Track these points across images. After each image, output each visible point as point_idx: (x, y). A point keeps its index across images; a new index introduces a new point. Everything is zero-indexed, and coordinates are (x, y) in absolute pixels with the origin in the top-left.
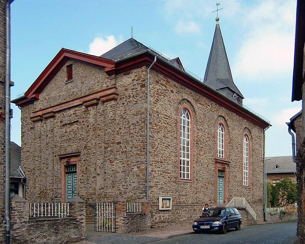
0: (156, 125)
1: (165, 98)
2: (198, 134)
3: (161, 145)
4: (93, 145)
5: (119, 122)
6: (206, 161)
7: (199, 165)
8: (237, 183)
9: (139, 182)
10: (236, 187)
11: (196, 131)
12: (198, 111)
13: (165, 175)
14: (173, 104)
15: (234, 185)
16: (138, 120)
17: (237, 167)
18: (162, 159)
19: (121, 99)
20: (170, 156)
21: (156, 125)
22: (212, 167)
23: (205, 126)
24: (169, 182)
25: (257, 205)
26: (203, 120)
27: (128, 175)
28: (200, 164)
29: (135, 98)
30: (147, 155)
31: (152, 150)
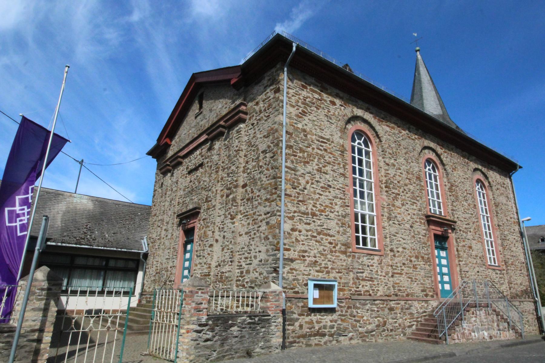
0: (302, 151)
1: (319, 111)
2: (387, 172)
3: (312, 184)
4: (214, 194)
5: (247, 153)
6: (409, 217)
7: (394, 223)
8: (475, 259)
9: (267, 251)
10: (474, 268)
11: (383, 167)
12: (385, 137)
13: (322, 239)
14: (334, 121)
15: (470, 262)
16: (269, 143)
17: (470, 232)
18: (314, 209)
19: (250, 119)
20: (331, 204)
21: (302, 151)
22: (421, 228)
23: (400, 161)
24: (331, 251)
25: (522, 302)
26: (394, 150)
27: (253, 238)
28: (397, 223)
29: (267, 111)
30: (280, 200)
31: (293, 192)
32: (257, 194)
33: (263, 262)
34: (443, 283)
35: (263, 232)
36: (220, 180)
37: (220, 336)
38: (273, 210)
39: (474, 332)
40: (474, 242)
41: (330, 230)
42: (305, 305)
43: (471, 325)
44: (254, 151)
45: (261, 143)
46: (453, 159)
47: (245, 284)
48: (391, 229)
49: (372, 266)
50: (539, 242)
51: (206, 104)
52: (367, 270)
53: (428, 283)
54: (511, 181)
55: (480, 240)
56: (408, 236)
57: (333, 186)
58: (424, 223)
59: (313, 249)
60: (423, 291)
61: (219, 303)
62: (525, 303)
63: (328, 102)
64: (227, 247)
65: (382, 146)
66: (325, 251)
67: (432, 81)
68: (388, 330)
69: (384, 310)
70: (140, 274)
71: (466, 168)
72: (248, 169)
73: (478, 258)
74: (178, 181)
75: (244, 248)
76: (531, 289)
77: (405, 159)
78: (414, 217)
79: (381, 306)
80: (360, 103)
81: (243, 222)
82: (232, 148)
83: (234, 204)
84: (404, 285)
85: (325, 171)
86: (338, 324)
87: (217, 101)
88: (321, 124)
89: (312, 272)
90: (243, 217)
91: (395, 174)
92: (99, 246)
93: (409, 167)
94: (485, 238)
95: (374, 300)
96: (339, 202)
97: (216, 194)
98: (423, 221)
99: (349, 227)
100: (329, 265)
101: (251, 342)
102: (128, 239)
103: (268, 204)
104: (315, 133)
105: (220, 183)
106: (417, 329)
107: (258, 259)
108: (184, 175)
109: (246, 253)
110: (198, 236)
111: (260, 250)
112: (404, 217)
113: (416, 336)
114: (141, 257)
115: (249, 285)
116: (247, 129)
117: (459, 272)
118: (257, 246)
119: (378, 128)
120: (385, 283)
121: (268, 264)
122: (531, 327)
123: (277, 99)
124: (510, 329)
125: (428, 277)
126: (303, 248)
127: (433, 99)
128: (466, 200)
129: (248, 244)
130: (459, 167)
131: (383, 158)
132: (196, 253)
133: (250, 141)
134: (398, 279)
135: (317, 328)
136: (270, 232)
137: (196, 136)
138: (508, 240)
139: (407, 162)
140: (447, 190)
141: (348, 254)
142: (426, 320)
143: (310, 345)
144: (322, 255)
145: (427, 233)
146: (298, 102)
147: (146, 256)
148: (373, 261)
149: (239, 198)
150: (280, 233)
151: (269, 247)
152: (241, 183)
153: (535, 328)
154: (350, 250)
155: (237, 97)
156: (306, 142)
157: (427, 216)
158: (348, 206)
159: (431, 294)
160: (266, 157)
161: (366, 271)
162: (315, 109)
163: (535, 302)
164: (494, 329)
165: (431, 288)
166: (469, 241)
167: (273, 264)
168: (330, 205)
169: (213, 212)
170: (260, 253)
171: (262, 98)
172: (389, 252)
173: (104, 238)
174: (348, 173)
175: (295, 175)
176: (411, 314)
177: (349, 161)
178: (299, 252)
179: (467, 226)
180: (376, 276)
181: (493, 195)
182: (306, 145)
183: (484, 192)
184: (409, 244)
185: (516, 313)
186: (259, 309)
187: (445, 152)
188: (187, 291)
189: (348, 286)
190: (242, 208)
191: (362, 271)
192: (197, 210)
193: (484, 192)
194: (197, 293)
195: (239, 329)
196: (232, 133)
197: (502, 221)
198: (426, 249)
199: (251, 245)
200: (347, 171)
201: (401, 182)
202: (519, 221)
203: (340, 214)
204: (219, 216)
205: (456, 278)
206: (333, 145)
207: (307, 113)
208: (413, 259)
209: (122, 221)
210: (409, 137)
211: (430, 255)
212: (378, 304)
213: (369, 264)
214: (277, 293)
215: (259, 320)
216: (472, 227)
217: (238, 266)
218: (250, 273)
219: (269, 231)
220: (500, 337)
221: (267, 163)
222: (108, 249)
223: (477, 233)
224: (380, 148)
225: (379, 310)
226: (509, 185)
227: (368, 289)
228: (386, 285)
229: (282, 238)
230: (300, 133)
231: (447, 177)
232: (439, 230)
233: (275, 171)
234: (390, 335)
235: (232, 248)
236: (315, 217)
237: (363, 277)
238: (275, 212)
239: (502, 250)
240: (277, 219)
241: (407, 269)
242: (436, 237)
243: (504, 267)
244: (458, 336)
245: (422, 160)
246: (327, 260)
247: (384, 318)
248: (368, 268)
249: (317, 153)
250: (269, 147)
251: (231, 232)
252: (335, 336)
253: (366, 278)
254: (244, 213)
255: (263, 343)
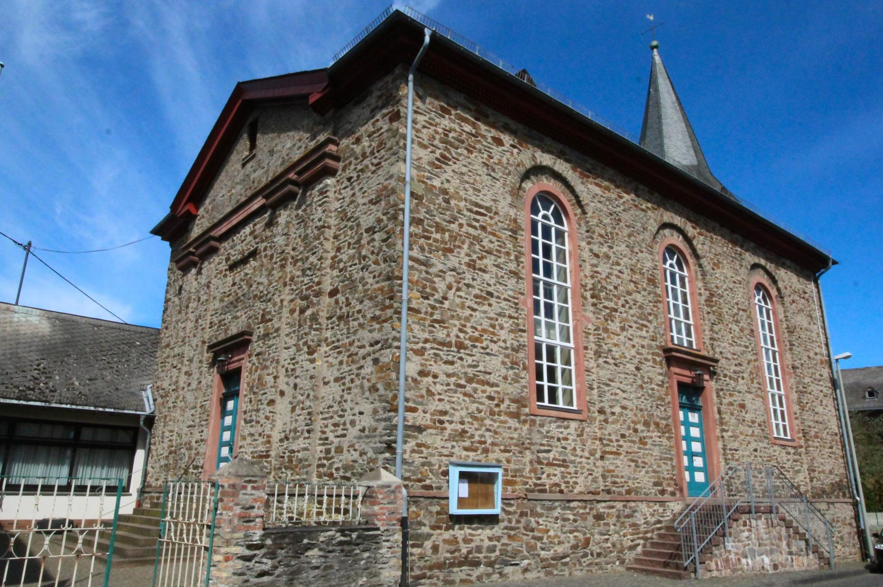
0: (439, 229)
1: (472, 156)
2: (595, 269)
3: (458, 289)
4: (277, 308)
5: (338, 233)
6: (633, 352)
7: (606, 362)
8: (750, 427)
9: (375, 412)
10: (749, 443)
12: (593, 204)
13: (475, 390)
14: (500, 174)
15: (741, 433)
16: (379, 214)
17: (743, 378)
18: (462, 335)
19: (344, 170)
20: (493, 326)
21: (439, 229)
22: (655, 371)
23: (619, 249)
24: (492, 413)
25: (833, 503)
26: (609, 230)
27: (349, 389)
29: (377, 154)
30: (399, 319)
32: (358, 308)
33: (367, 432)
34: (692, 469)
35: (367, 377)
36: (288, 282)
37: (287, 565)
38: (386, 337)
39: (746, 557)
40: (749, 396)
41: (490, 373)
42: (444, 510)
43: (740, 544)
44: (351, 228)
45: (365, 213)
46: (713, 246)
47: (334, 471)
48: (601, 373)
49: (566, 439)
50: (864, 397)
51: (262, 141)
52: (557, 447)
53: (665, 470)
54: (817, 287)
55: (759, 393)
56: (632, 385)
57: (496, 294)
58: (661, 362)
59: (459, 408)
60: (656, 484)
61: (285, 506)
62: (837, 505)
63: (490, 140)
64: (301, 405)
65: (588, 222)
66: (480, 411)
67: (680, 104)
68: (592, 555)
69: (585, 519)
70: (140, 455)
71: (738, 263)
72: (341, 260)
73: (756, 425)
74: (210, 282)
75: (332, 407)
76: (849, 481)
77: (627, 246)
78: (644, 351)
79: (581, 511)
80: (549, 141)
81: (330, 359)
82: (311, 224)
83: (314, 326)
84: (623, 474)
85: (483, 267)
86: (503, 544)
87: (282, 136)
88: (475, 180)
89: (456, 450)
90: (331, 349)
91: (610, 274)
92: (61, 403)
93: (634, 261)
94: (769, 389)
95: (569, 501)
96: (507, 324)
97: (281, 307)
98: (658, 359)
99: (525, 368)
100: (487, 438)
101: (343, 576)
102: (117, 389)
103: (377, 326)
104: (464, 196)
105: (288, 287)
106: (645, 553)
107: (358, 427)
108: (221, 271)
109: (336, 416)
110: (248, 384)
111: (362, 410)
112: (625, 351)
113: (641, 564)
114: (142, 423)
115: (341, 473)
116: (338, 188)
117: (722, 451)
118: (357, 404)
119: (579, 188)
120: (588, 470)
121: (375, 436)
122: (847, 549)
123: (395, 133)
124: (810, 553)
125: (665, 459)
126: (441, 407)
127: (680, 137)
128: (737, 321)
129: (339, 399)
130: (725, 262)
131: (589, 243)
132: (244, 416)
133: (345, 210)
134: (613, 463)
135: (464, 551)
136: (380, 378)
137: (243, 199)
138: (810, 393)
139: (632, 251)
140: (703, 302)
141: (523, 418)
142: (660, 536)
143: (452, 582)
144: (476, 419)
145: (666, 379)
146: (434, 138)
147: (150, 420)
148: (568, 431)
149: (324, 314)
150: (398, 379)
151: (377, 404)
152: (329, 288)
153: (853, 550)
154: (527, 410)
155: (321, 127)
156: (448, 213)
157: (667, 350)
158: (524, 331)
159: (670, 489)
160: (373, 240)
161: (555, 449)
162: (465, 152)
163: (855, 505)
164: (781, 553)
165: (671, 479)
166: (741, 395)
167: (385, 435)
168: (491, 329)
169: (274, 341)
170: (361, 416)
171: (366, 131)
172: (597, 414)
173: (70, 387)
174: (524, 271)
175: (427, 273)
176: (634, 525)
177: (527, 247)
178: (432, 414)
179: (738, 369)
180: (573, 458)
181: (785, 312)
182: (447, 218)
183: (770, 307)
184: (634, 399)
185: (821, 524)
186: (358, 518)
187: (700, 234)
188: (226, 485)
189: (522, 476)
190: (329, 334)
191: (546, 448)
192: (246, 337)
193: (770, 307)
194: (244, 488)
195: (321, 553)
196: (311, 195)
197: (800, 359)
198: (663, 409)
199: (346, 401)
200: (523, 267)
201: (621, 288)
202: (830, 360)
203: (508, 345)
204: (285, 348)
205: (715, 462)
206: (497, 218)
207: (450, 160)
208: (640, 427)
209: (105, 356)
210: (636, 206)
211: (670, 421)
212: (575, 508)
213: (561, 436)
214: (393, 488)
215: (359, 537)
216: (747, 369)
217: (321, 439)
218: (342, 452)
219: (379, 375)
220: (792, 566)
221: (376, 251)
222: (80, 407)
223: (755, 381)
224: (583, 225)
225: (578, 518)
226: (815, 294)
227: (557, 481)
228: (591, 474)
229: (402, 387)
230: (437, 195)
231: (704, 279)
232: (686, 375)
233: (390, 266)
234: (597, 564)
235: (310, 407)
236: (462, 351)
237: (548, 459)
238: (390, 341)
239: (798, 412)
240: (394, 353)
241: (629, 444)
242: (682, 386)
243: (802, 442)
244: (717, 564)
245: (659, 248)
246: (484, 429)
247: (585, 534)
248: (558, 444)
249: (467, 233)
250: (379, 221)
251: (309, 376)
252: (497, 566)
253: (555, 462)
254: (333, 342)
255: (365, 579)
